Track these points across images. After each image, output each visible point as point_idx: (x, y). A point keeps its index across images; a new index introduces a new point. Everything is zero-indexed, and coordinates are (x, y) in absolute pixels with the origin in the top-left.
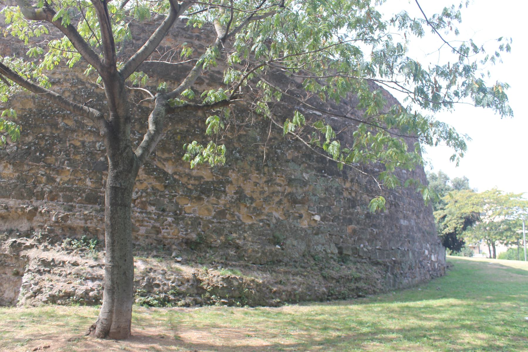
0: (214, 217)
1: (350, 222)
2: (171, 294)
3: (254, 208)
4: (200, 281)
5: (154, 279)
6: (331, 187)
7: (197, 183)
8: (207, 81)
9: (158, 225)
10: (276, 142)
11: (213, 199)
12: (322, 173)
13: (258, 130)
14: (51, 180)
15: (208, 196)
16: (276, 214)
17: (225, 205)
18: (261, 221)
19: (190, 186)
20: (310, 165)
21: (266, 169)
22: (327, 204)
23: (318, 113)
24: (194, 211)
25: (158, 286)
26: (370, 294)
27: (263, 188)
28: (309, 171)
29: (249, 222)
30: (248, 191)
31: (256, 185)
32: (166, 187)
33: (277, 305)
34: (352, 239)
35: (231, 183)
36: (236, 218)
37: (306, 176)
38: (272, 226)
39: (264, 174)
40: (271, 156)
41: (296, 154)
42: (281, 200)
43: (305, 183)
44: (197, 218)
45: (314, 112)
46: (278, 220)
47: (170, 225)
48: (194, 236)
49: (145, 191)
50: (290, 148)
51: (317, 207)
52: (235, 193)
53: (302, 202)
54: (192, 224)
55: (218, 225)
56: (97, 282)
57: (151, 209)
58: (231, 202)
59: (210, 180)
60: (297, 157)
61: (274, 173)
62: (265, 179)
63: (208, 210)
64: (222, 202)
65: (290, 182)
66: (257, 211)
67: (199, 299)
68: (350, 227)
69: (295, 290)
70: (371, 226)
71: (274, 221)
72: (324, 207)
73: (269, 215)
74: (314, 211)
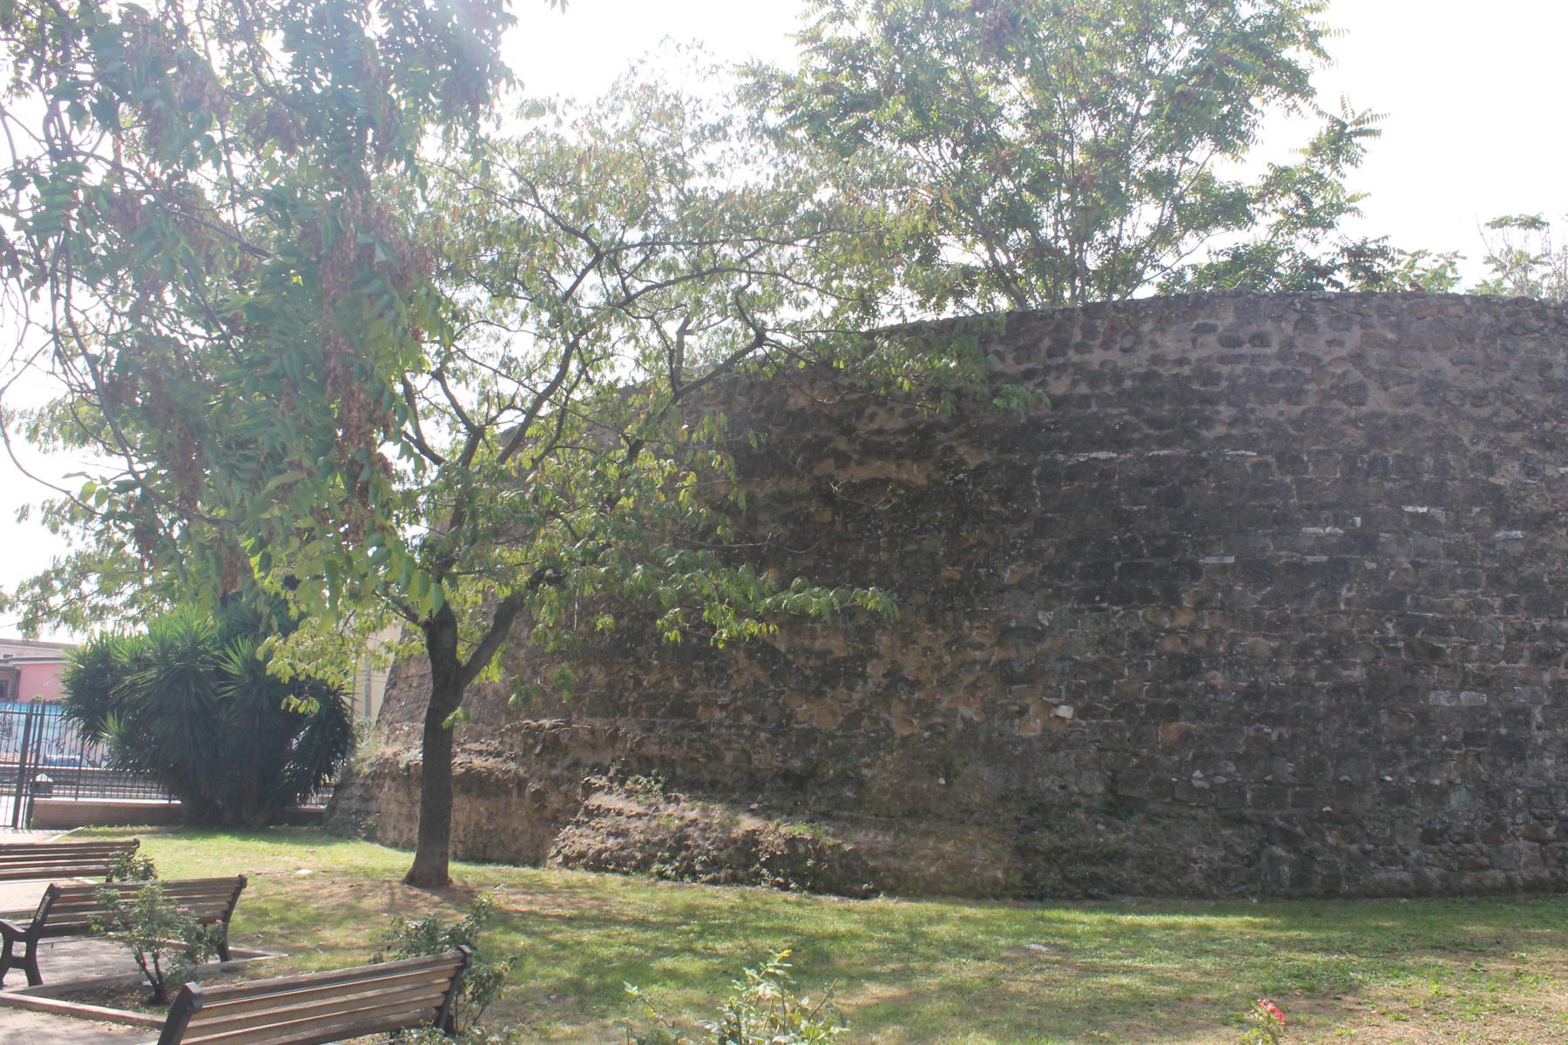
0: (841, 727)
1: (1173, 714)
2: (702, 862)
3: (919, 701)
4: (756, 843)
5: (687, 837)
6: (1118, 633)
7: (819, 663)
8: (856, 457)
9: (748, 747)
10: (983, 551)
11: (842, 691)
12: (1094, 602)
13: (944, 534)
14: (638, 683)
15: (833, 688)
16: (965, 711)
17: (861, 701)
18: (930, 728)
19: (808, 672)
20: (1060, 588)
21: (949, 616)
22: (1100, 676)
23: (1103, 455)
24: (811, 717)
25: (688, 847)
26: (1134, 895)
27: (940, 658)
28: (1055, 603)
29: (902, 731)
30: (909, 671)
31: (925, 655)
32: (772, 677)
33: (866, 896)
34: (1176, 758)
35: (877, 655)
36: (882, 725)
37: (1044, 618)
38: (951, 736)
39: (945, 628)
40: (966, 584)
41: (1030, 569)
42: (978, 679)
43: (1038, 635)
44: (813, 730)
45: (1094, 455)
46: (968, 722)
47: (763, 747)
48: (797, 764)
49: (743, 689)
50: (1014, 559)
51: (1068, 688)
52: (885, 676)
53: (1031, 677)
54: (797, 743)
55: (843, 741)
56: (620, 840)
57: (748, 718)
58: (875, 694)
59: (844, 654)
60: (1031, 576)
61: (967, 623)
62: (945, 640)
63: (833, 714)
64: (856, 696)
65: (1004, 634)
66: (924, 709)
67: (741, 873)
68: (1173, 726)
69: (918, 869)
70: (1258, 720)
71: (960, 726)
72: (1089, 685)
73: (951, 714)
74: (1059, 696)
